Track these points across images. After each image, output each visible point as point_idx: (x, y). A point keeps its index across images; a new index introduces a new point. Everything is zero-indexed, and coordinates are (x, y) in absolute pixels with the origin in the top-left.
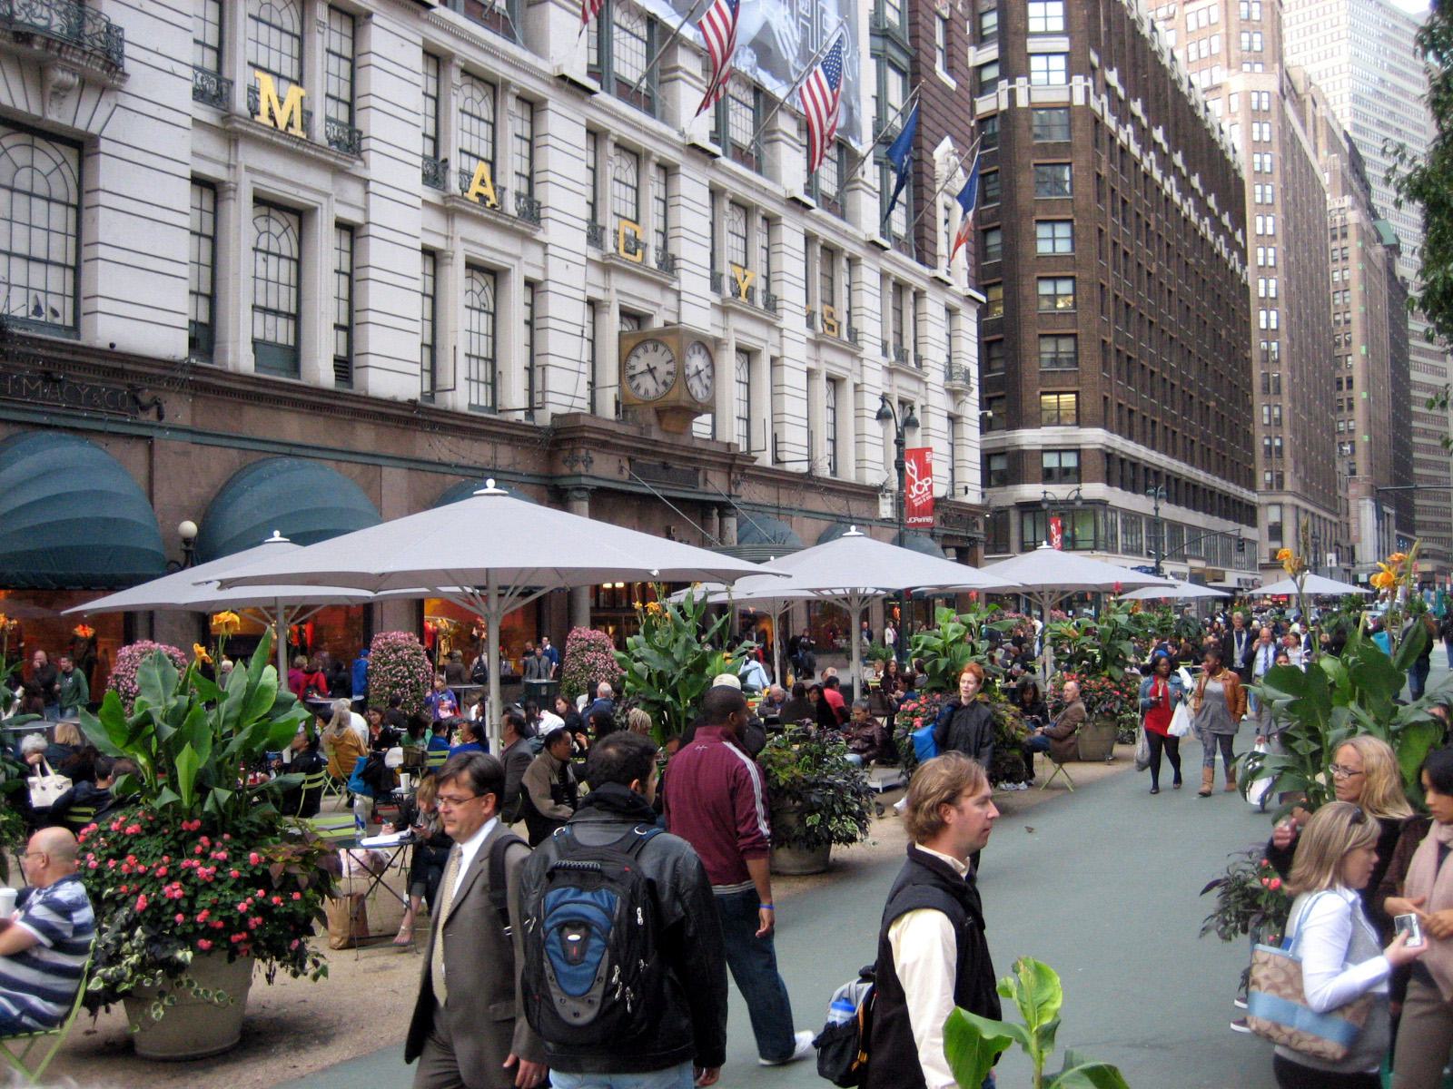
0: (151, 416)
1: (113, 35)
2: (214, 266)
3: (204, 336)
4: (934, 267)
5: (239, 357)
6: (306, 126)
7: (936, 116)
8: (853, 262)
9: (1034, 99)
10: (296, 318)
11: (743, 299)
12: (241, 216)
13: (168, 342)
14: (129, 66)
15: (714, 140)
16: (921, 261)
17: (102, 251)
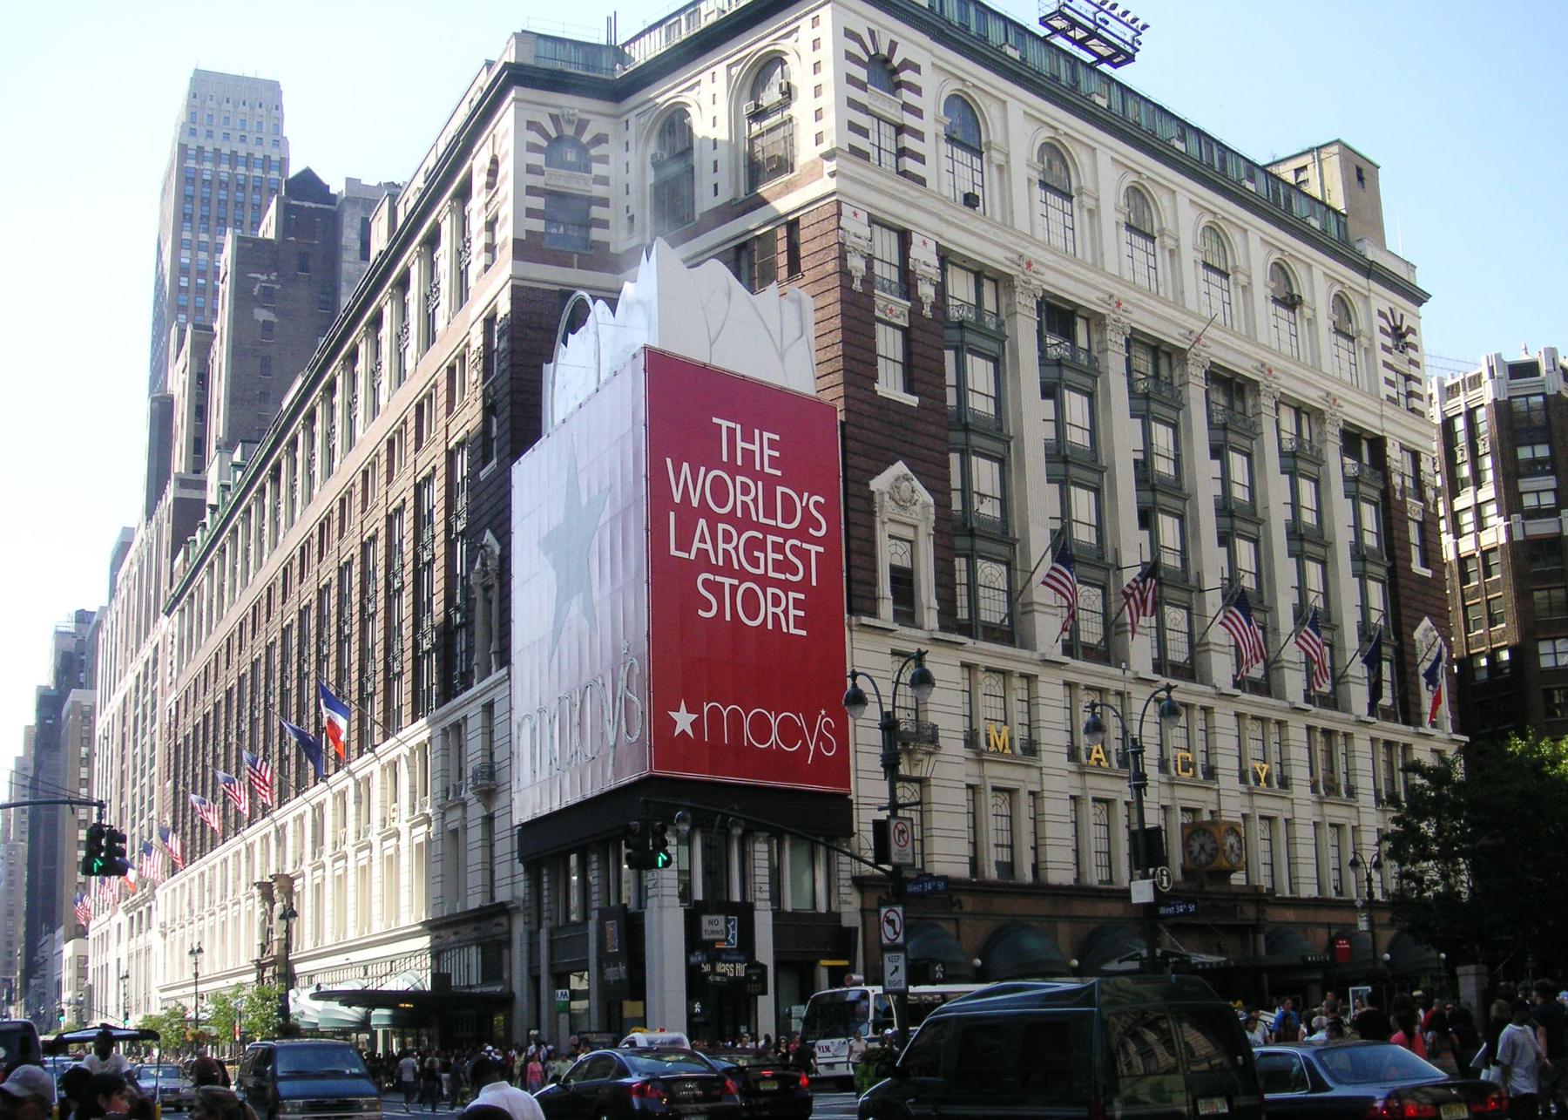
0: (956, 909)
1: (935, 728)
2: (974, 828)
3: (974, 863)
4: (1420, 724)
5: (992, 873)
6: (1011, 747)
7: (1414, 604)
8: (1347, 736)
9: (1528, 533)
10: (1011, 847)
11: (1263, 784)
12: (990, 801)
13: (962, 871)
14: (941, 741)
15: (1237, 685)
16: (1406, 722)
17: (934, 832)
